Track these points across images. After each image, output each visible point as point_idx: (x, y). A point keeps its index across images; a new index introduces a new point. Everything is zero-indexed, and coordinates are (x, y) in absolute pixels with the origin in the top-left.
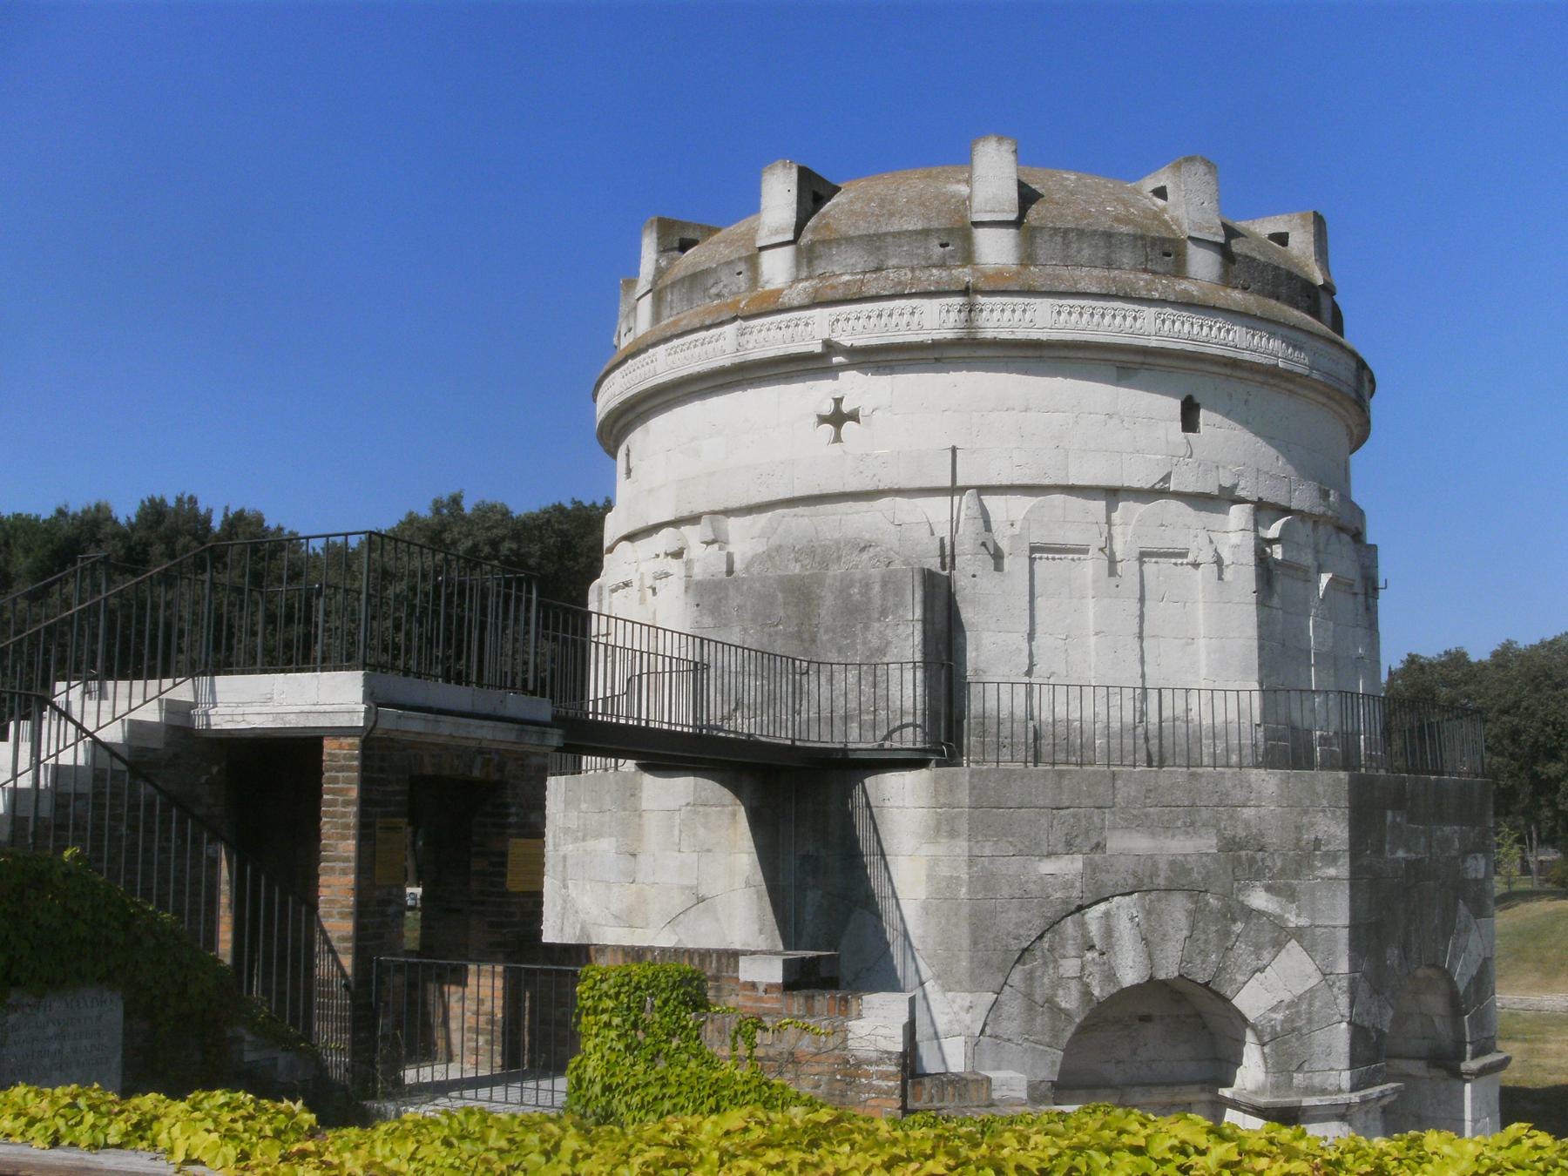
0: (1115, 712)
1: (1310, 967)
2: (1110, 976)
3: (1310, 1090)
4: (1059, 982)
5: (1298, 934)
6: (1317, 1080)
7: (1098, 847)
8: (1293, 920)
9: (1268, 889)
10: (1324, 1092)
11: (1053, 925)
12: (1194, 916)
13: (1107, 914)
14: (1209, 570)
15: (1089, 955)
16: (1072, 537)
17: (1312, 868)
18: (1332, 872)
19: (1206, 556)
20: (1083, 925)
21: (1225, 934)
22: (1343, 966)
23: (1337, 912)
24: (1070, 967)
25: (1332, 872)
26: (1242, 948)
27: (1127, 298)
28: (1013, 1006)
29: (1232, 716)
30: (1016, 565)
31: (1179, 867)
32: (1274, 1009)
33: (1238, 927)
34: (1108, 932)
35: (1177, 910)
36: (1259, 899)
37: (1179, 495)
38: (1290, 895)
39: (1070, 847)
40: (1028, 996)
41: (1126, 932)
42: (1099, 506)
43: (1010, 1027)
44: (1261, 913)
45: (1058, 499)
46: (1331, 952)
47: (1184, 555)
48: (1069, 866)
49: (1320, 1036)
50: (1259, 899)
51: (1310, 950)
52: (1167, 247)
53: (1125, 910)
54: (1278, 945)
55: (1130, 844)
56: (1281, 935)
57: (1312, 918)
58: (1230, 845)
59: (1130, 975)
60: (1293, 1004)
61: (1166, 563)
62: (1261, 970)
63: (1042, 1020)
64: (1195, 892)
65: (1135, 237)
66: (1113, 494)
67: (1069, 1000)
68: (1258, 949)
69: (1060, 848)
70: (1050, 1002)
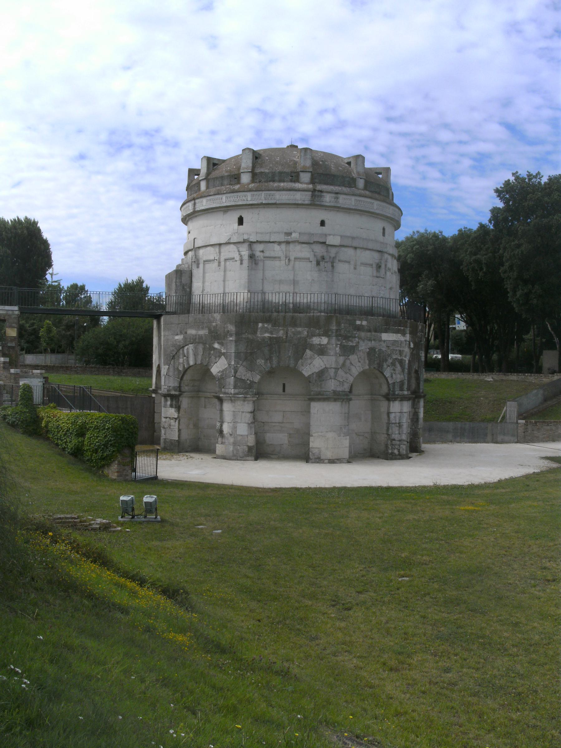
0: (216, 300)
1: (226, 362)
2: (188, 363)
3: (225, 393)
4: (179, 364)
5: (224, 354)
6: (227, 391)
7: (186, 333)
8: (223, 351)
9: (218, 343)
10: (228, 394)
11: (178, 351)
12: (204, 349)
13: (188, 348)
14: (239, 262)
15: (185, 358)
16: (212, 258)
17: (227, 338)
18: (231, 339)
19: (237, 258)
20: (183, 351)
21: (210, 354)
22: (233, 363)
23: (232, 349)
24: (181, 360)
25: (231, 339)
26: (213, 357)
27: (218, 194)
28: (171, 369)
29: (242, 300)
30: (201, 266)
31: (201, 337)
32: (218, 372)
33: (212, 352)
34: (188, 352)
35: (200, 348)
36: (216, 346)
37: (234, 243)
38: (221, 344)
39: (181, 333)
40: (174, 367)
41: (191, 352)
42: (217, 249)
43: (171, 374)
44: (217, 349)
45: (209, 248)
46: (230, 359)
47: (234, 258)
48: (179, 337)
49: (228, 380)
50: (216, 346)
51: (226, 358)
52: (236, 176)
53: (191, 347)
54: (220, 357)
55: (192, 332)
56: (220, 354)
57: (227, 350)
58: (210, 332)
59: (191, 363)
60: (222, 371)
61: (231, 261)
62: (216, 363)
63: (176, 373)
64: (205, 344)
65: (228, 176)
66: (220, 245)
67: (181, 368)
68: (216, 357)
69: (179, 333)
70: (178, 368)
